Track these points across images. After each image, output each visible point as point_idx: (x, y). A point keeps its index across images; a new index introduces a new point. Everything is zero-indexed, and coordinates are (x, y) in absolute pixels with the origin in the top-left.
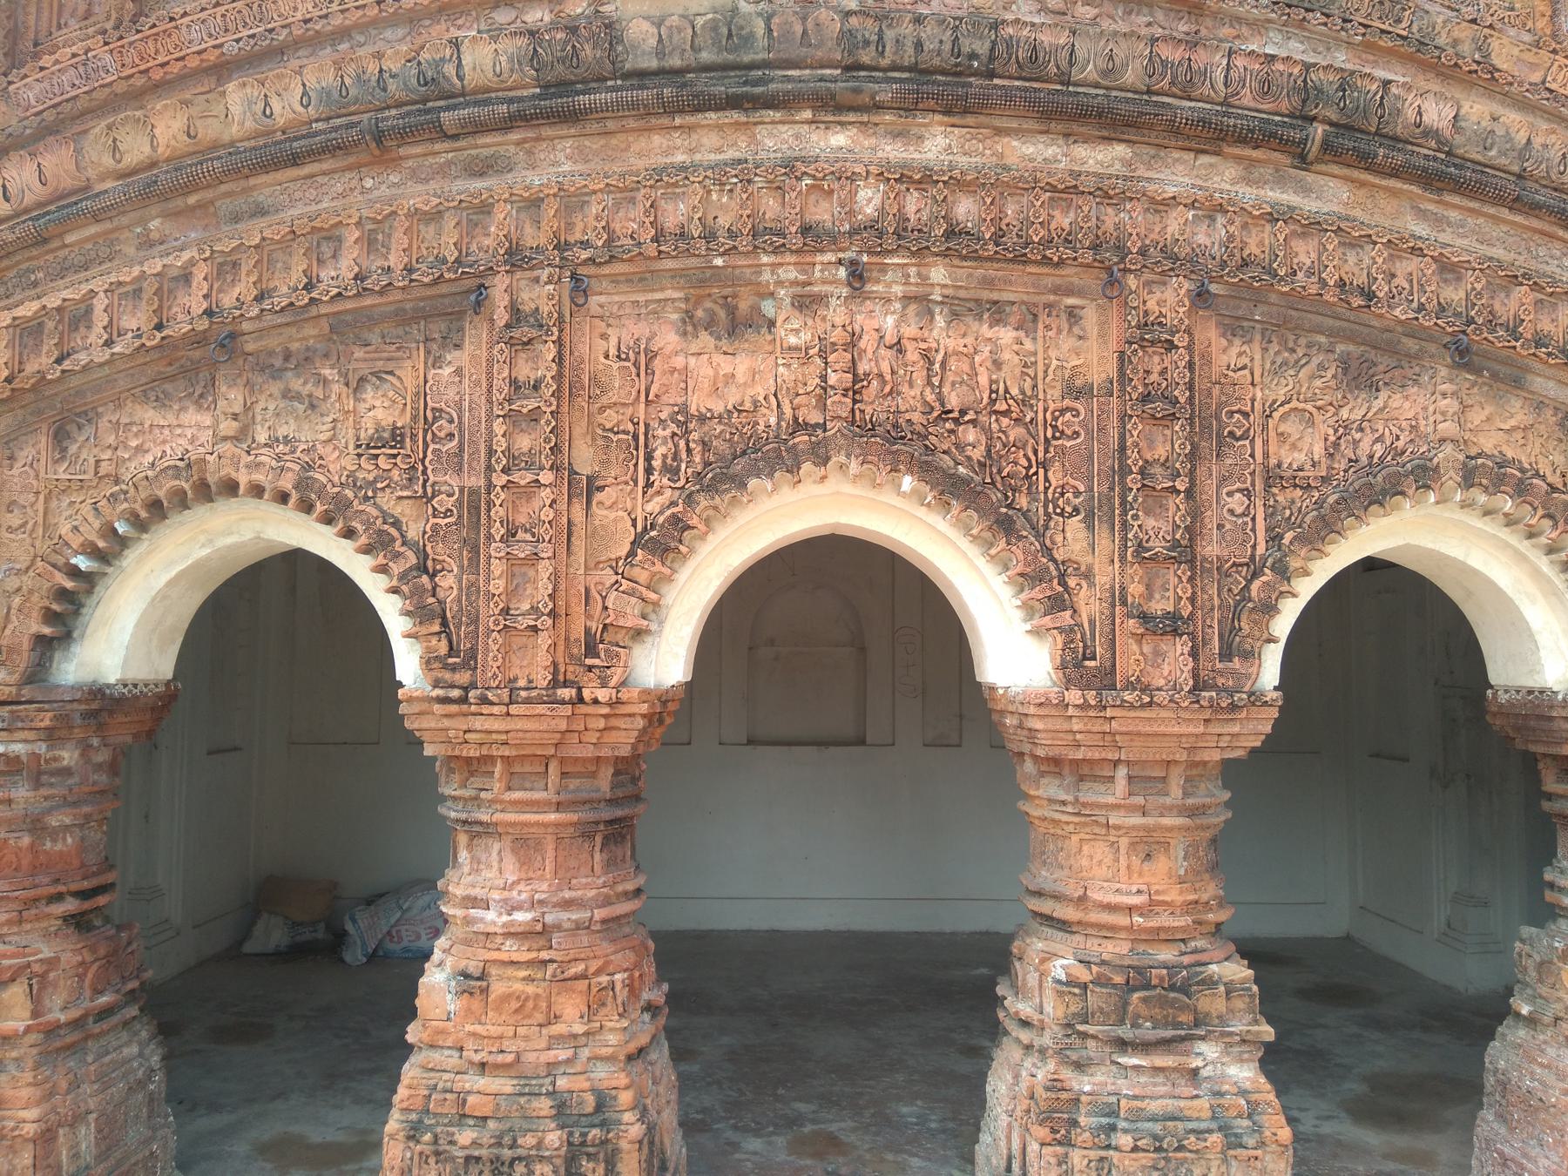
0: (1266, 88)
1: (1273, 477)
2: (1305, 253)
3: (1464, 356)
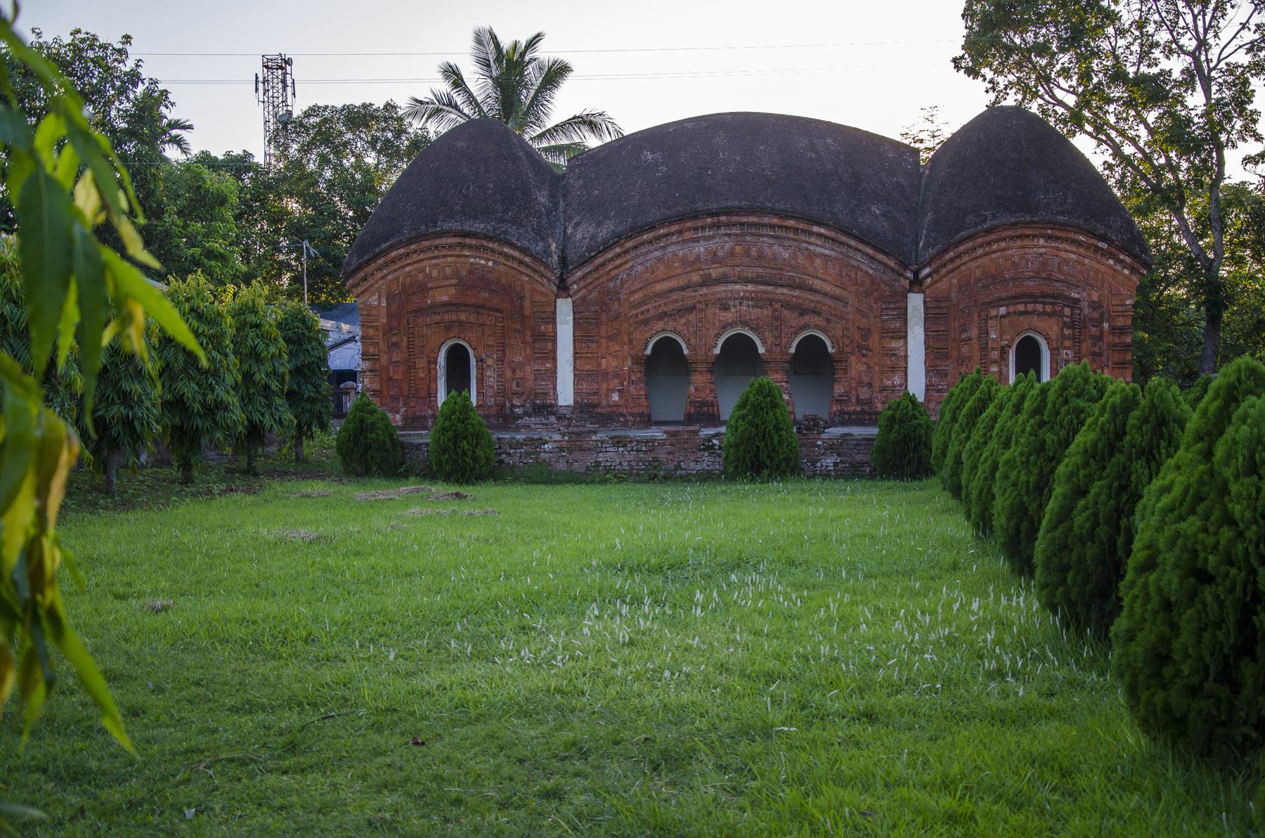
3: (814, 312)
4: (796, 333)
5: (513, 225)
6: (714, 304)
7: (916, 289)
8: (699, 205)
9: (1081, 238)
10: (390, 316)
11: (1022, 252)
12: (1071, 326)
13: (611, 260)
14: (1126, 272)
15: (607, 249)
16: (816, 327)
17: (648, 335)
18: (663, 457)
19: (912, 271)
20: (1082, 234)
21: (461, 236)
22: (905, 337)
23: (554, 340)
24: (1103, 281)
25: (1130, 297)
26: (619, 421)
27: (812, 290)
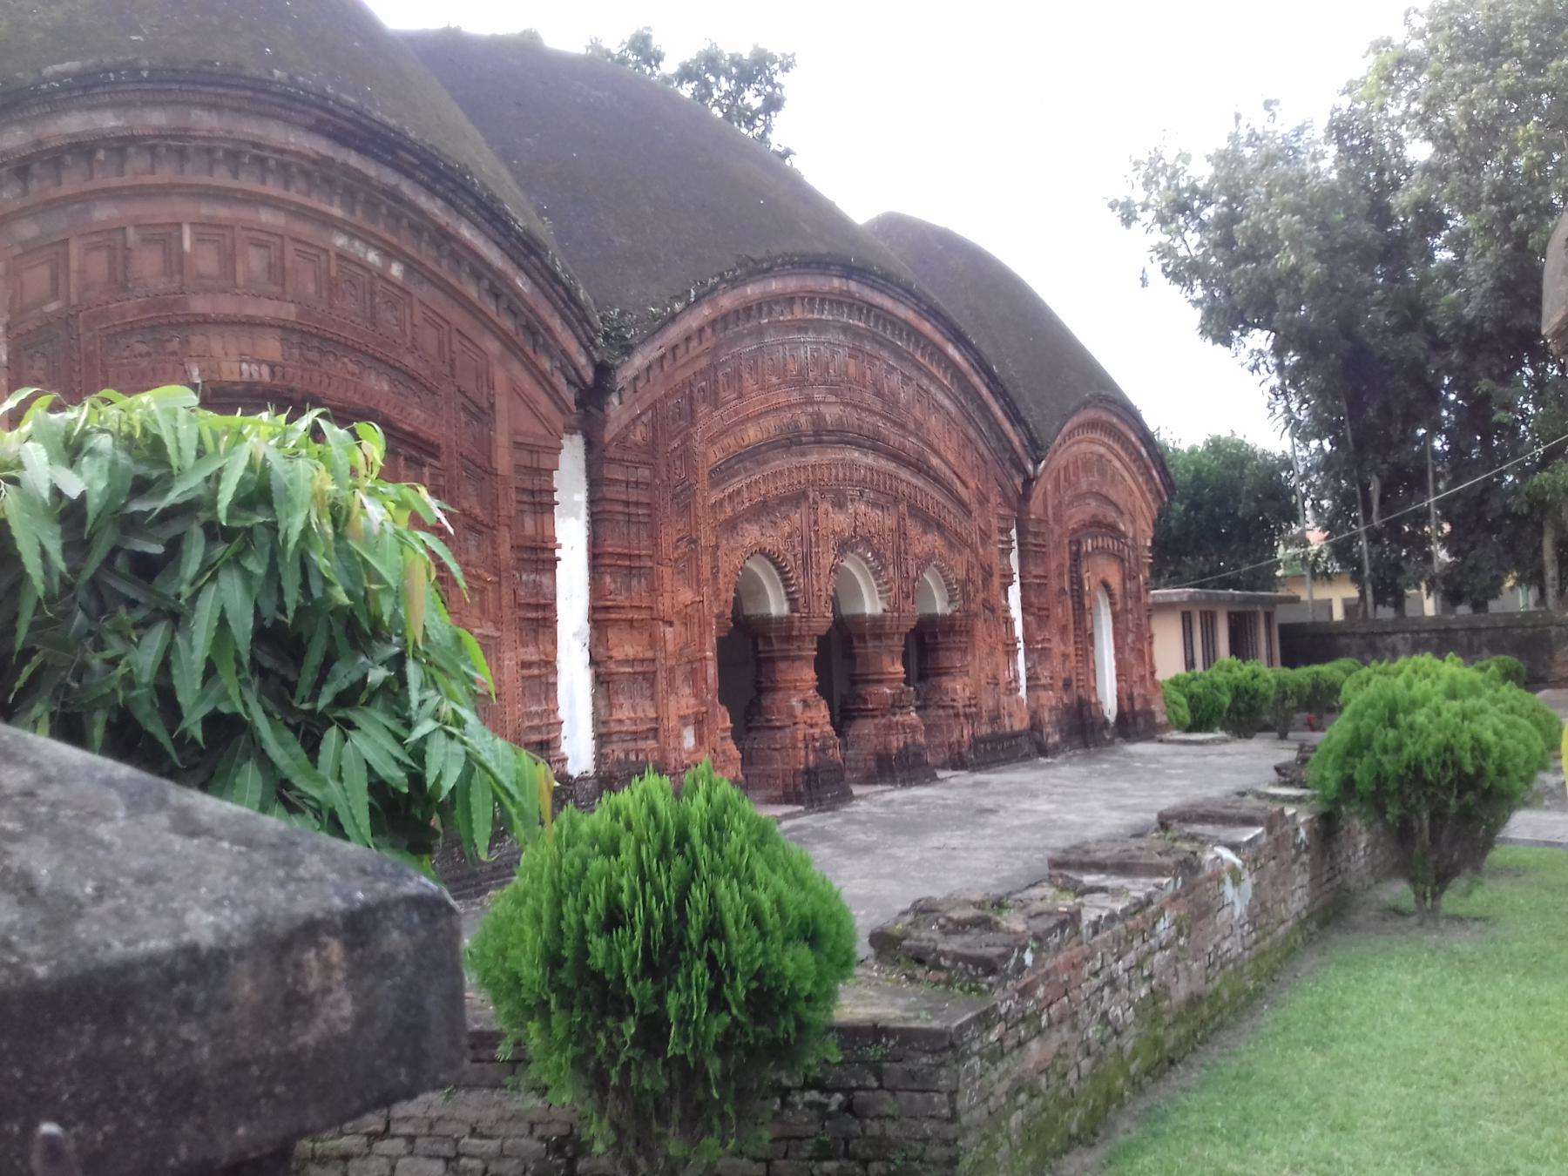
1: (916, 556)
21: (340, 137)
27: (937, 480)
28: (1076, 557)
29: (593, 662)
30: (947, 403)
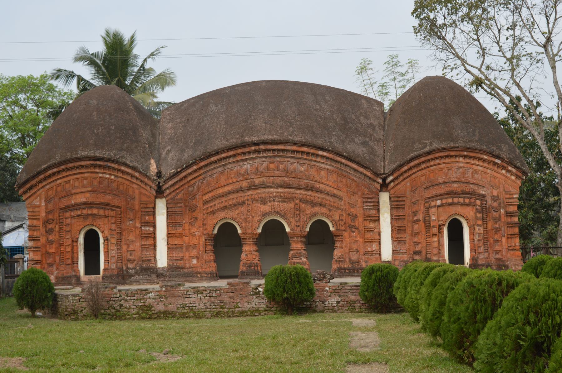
0: (305, 185)
2: (308, 197)
3: (320, 205)
4: (310, 219)
5: (127, 152)
6: (257, 200)
7: (384, 190)
8: (247, 139)
9: (485, 157)
10: (48, 213)
11: (449, 165)
12: (482, 211)
13: (190, 174)
14: (513, 178)
15: (188, 167)
16: (323, 214)
17: (215, 221)
18: (227, 300)
19: (382, 178)
20: (485, 155)
22: (378, 220)
23: (154, 226)
24: (500, 184)
25: (516, 194)
26: (197, 277)
27: (319, 191)
28: (428, 208)
29: (168, 244)
30: (328, 167)
